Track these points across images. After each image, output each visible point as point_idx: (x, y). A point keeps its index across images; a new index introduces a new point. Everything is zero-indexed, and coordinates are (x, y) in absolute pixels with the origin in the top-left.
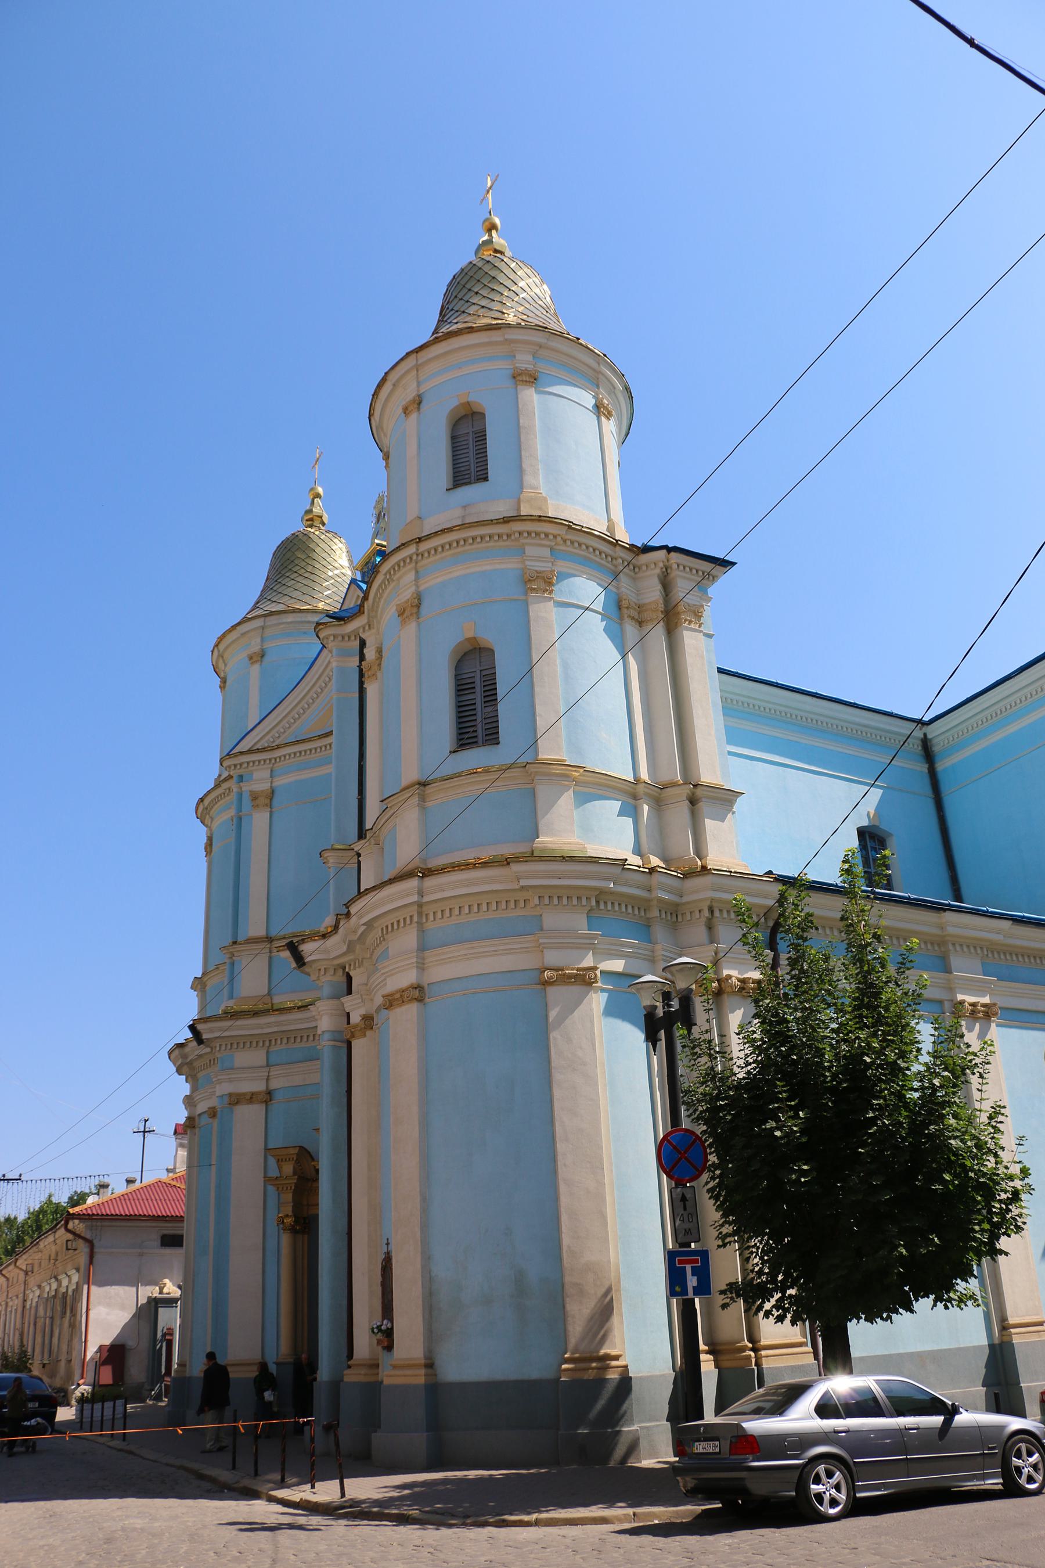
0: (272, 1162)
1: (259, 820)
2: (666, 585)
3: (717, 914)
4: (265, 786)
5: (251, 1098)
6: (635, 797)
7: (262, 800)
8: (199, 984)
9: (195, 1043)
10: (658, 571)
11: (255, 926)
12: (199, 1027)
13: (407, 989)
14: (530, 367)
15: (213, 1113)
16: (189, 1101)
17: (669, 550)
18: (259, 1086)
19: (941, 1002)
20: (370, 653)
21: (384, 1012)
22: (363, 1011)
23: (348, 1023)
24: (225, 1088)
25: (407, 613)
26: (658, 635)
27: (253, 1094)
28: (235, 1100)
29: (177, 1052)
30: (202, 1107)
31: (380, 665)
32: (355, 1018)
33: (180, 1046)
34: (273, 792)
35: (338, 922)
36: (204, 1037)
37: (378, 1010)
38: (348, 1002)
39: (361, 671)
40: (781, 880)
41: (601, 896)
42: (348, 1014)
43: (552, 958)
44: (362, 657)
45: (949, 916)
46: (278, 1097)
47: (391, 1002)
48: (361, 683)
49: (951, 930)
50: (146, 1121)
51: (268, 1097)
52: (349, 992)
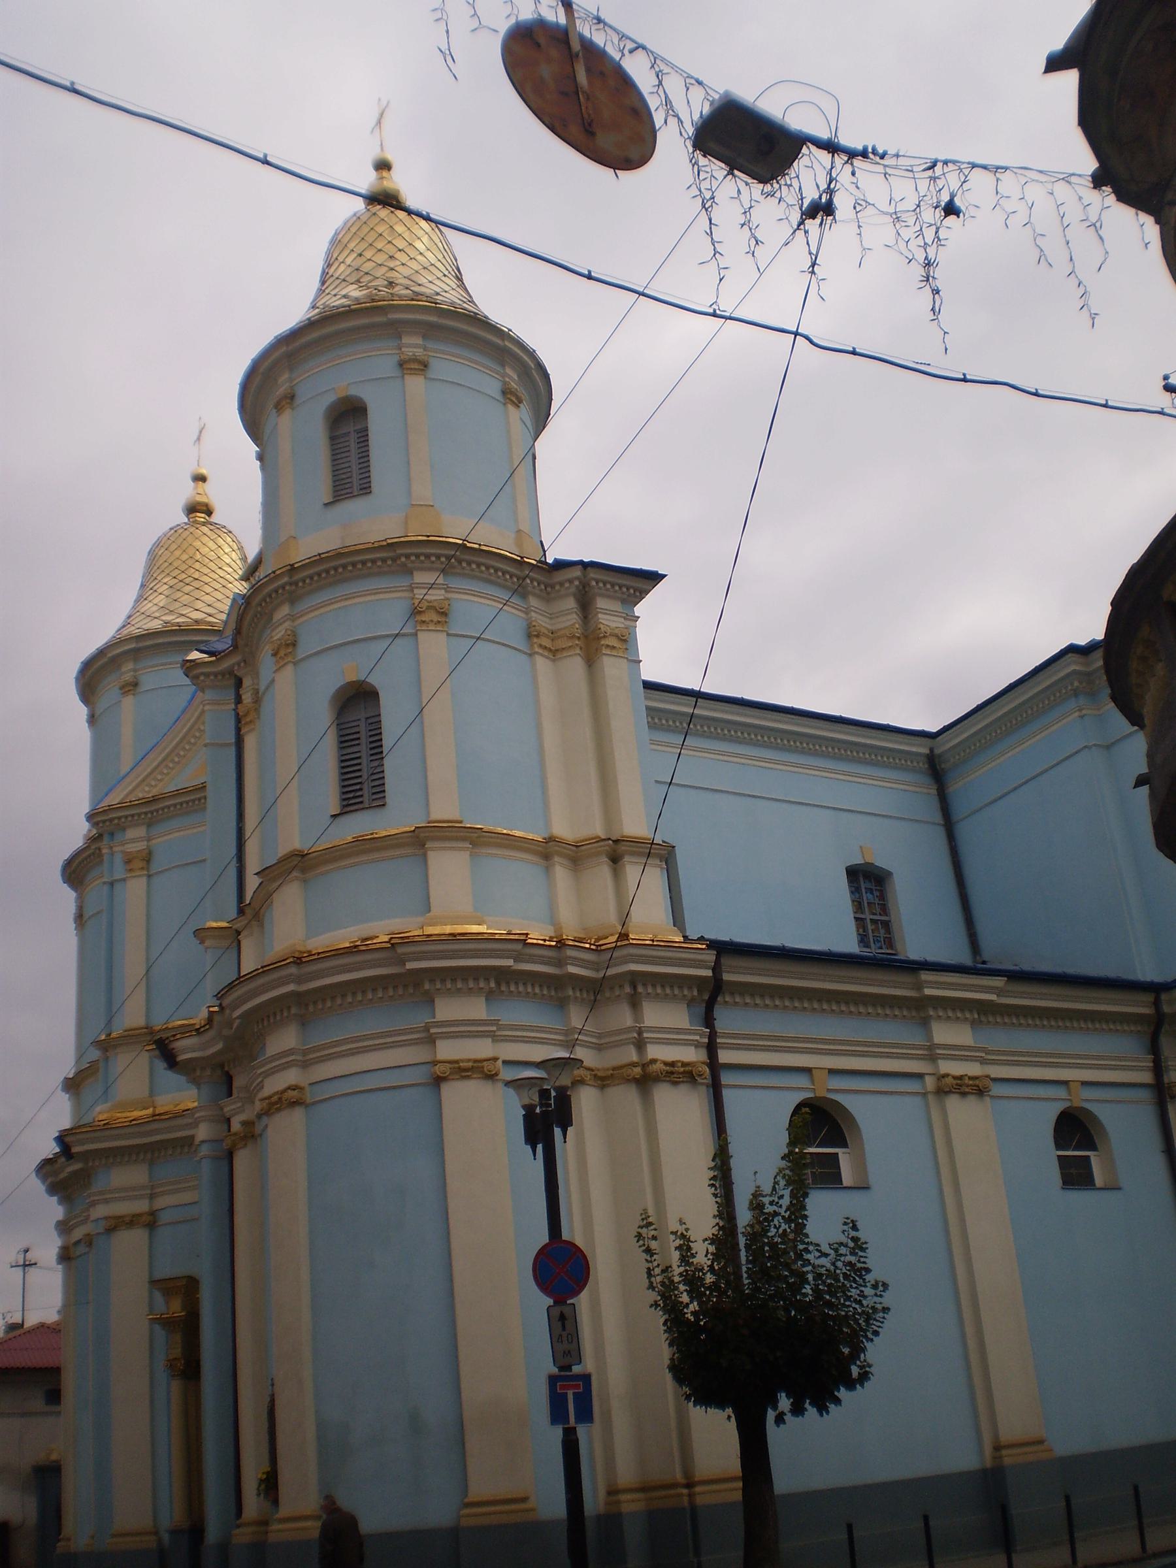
0: (158, 1297)
1: (136, 888)
2: (585, 606)
3: (640, 989)
4: (142, 845)
5: (131, 1222)
6: (547, 857)
7: (138, 864)
8: (73, 1085)
9: (63, 1159)
10: (573, 590)
11: (133, 1016)
12: (67, 1139)
14: (419, 352)
15: (89, 1240)
16: (64, 1227)
18: (142, 1206)
19: (920, 1076)
24: (100, 1211)
26: (575, 665)
27: (133, 1216)
29: (48, 1168)
30: (78, 1234)
32: (236, 1126)
33: (47, 1162)
34: (150, 853)
35: (211, 1013)
36: (75, 1150)
37: (259, 1116)
38: (229, 1107)
40: (714, 945)
41: (503, 976)
42: (228, 1120)
43: (448, 1050)
45: (925, 976)
46: (164, 1217)
49: (928, 992)
50: (26, 1251)
51: (151, 1222)
52: (230, 1094)
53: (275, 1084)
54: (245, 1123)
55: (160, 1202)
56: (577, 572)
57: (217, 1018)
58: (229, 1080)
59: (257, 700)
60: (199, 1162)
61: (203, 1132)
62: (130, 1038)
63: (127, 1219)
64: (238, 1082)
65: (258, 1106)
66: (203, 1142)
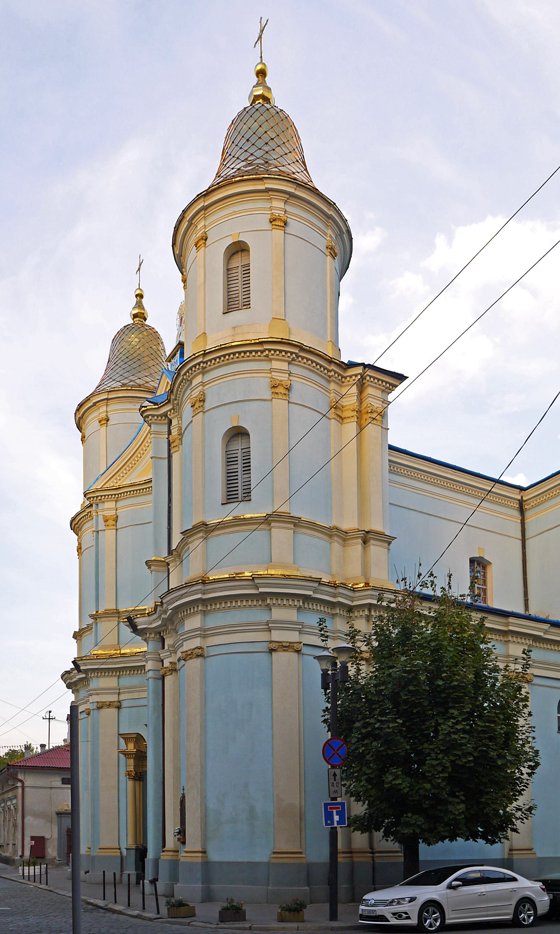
5: (109, 705)
13: (195, 649)
17: (365, 366)
18: (114, 698)
20: (174, 432)
21: (182, 662)
22: (170, 660)
23: (163, 666)
25: (197, 406)
27: (110, 702)
28: (101, 706)
31: (181, 440)
32: (166, 664)
34: (117, 517)
39: (169, 441)
42: (162, 661)
44: (170, 433)
46: (124, 704)
47: (188, 656)
48: (169, 450)
53: (189, 645)
54: (171, 663)
55: (122, 697)
56: (359, 370)
57: (159, 609)
58: (163, 640)
59: (181, 434)
60: (148, 680)
61: (149, 665)
62: (108, 614)
63: (108, 703)
64: (168, 642)
65: (179, 654)
66: (149, 670)
